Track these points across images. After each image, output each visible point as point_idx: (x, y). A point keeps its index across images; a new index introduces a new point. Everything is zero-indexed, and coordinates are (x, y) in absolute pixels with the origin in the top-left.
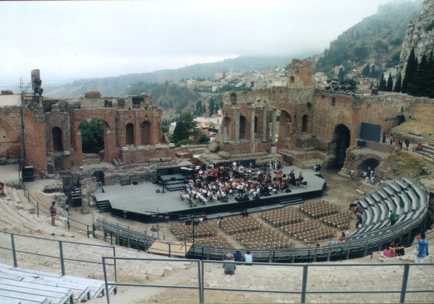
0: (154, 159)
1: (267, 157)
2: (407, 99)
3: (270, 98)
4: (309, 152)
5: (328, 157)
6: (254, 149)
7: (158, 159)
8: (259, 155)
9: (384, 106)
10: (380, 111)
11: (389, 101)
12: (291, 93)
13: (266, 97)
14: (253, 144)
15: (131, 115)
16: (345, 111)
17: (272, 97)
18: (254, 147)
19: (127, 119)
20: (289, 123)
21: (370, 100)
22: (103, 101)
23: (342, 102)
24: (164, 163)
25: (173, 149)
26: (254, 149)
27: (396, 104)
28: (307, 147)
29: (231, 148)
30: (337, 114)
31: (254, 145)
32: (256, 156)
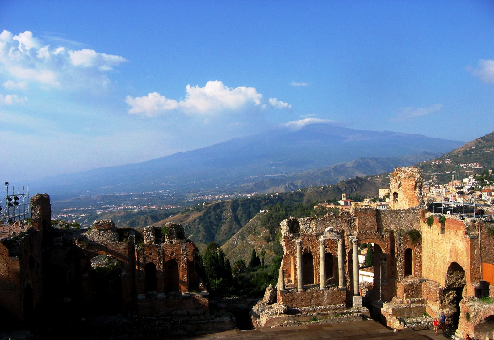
1: (345, 311)
3: (350, 226)
4: (414, 305)
5: (440, 312)
6: (325, 300)
8: (335, 309)
13: (344, 224)
14: (323, 291)
16: (456, 241)
17: (353, 225)
20: (383, 262)
23: (453, 228)
24: (193, 318)
26: (325, 300)
28: (412, 296)
29: (291, 298)
30: (448, 248)
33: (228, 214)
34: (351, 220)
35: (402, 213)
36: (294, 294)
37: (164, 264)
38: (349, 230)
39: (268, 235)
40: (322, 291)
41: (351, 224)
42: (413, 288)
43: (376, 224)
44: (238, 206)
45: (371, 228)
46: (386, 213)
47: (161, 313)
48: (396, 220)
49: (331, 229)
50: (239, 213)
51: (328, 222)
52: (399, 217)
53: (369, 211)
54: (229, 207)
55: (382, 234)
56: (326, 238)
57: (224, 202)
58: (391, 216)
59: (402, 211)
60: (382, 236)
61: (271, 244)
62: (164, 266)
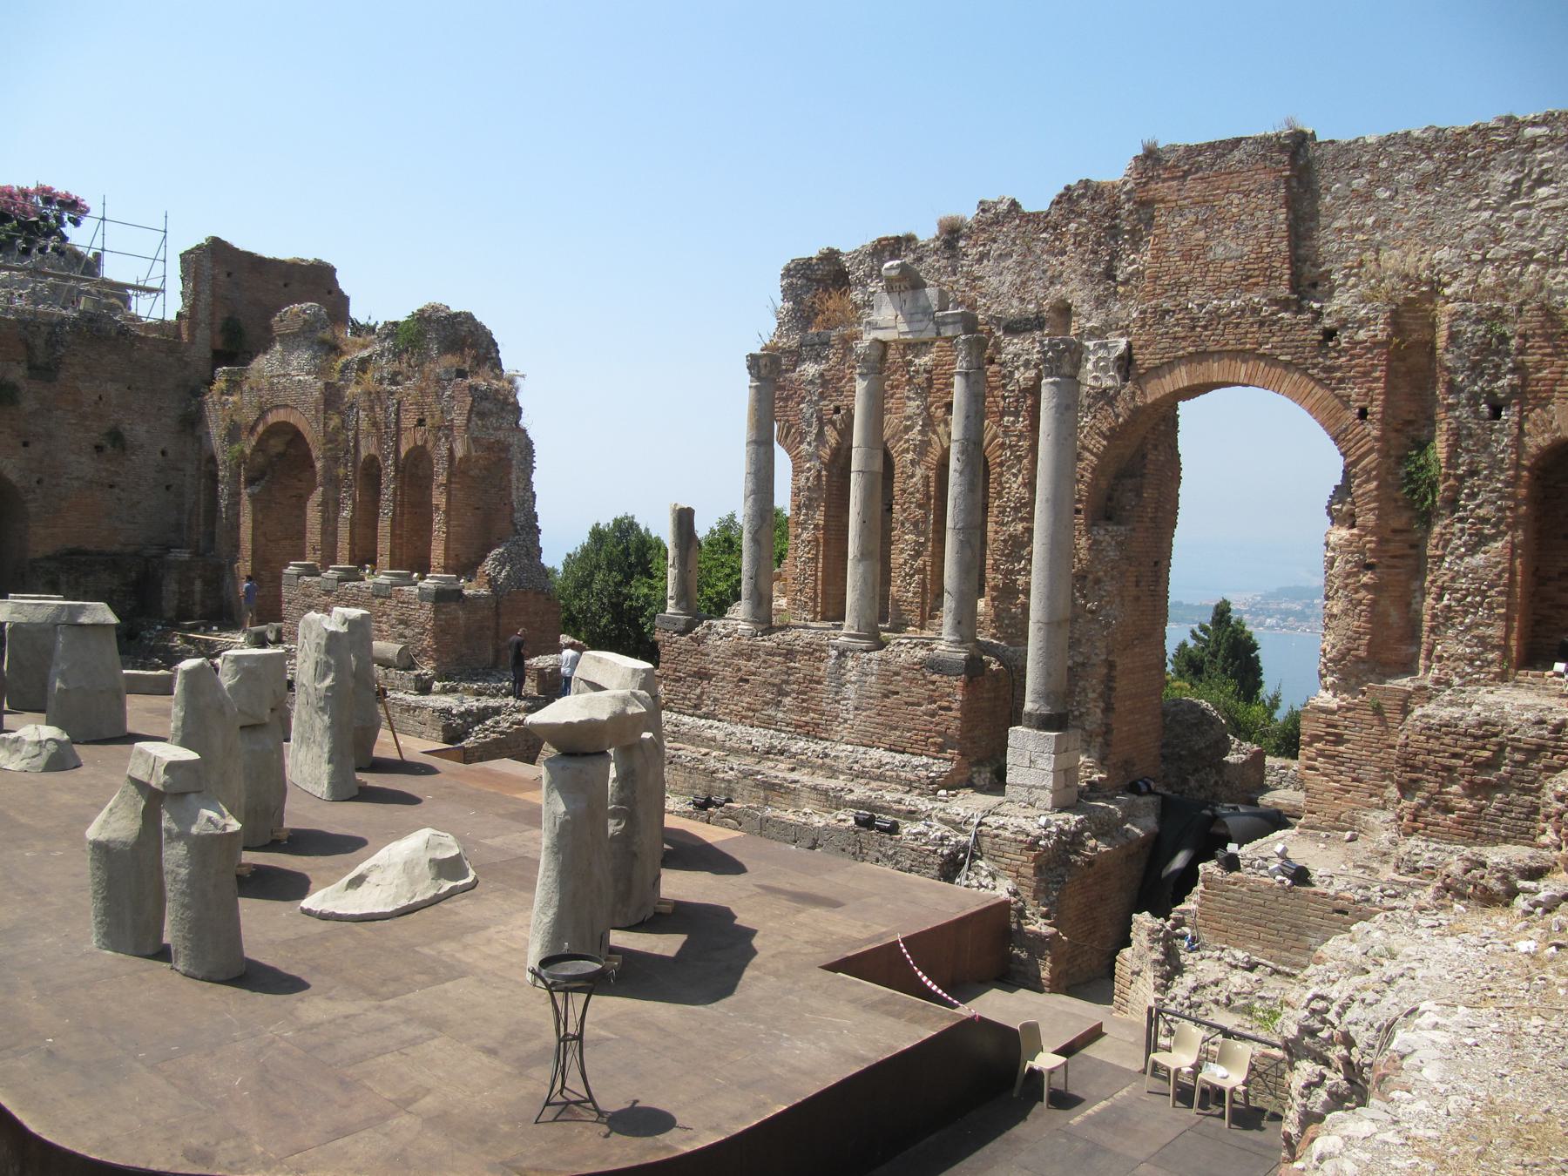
3: (1109, 274)
12: (1366, 197)
17: (1124, 270)
18: (850, 691)
29: (692, 664)
31: (852, 676)
32: (833, 773)
35: (1534, 144)
36: (712, 640)
37: (396, 463)
38: (1100, 303)
40: (834, 653)
41: (1115, 256)
43: (1284, 246)
45: (1245, 281)
46: (1383, 165)
48: (1475, 202)
49: (891, 268)
52: (1502, 178)
56: (880, 335)
59: (1529, 132)
62: (396, 470)
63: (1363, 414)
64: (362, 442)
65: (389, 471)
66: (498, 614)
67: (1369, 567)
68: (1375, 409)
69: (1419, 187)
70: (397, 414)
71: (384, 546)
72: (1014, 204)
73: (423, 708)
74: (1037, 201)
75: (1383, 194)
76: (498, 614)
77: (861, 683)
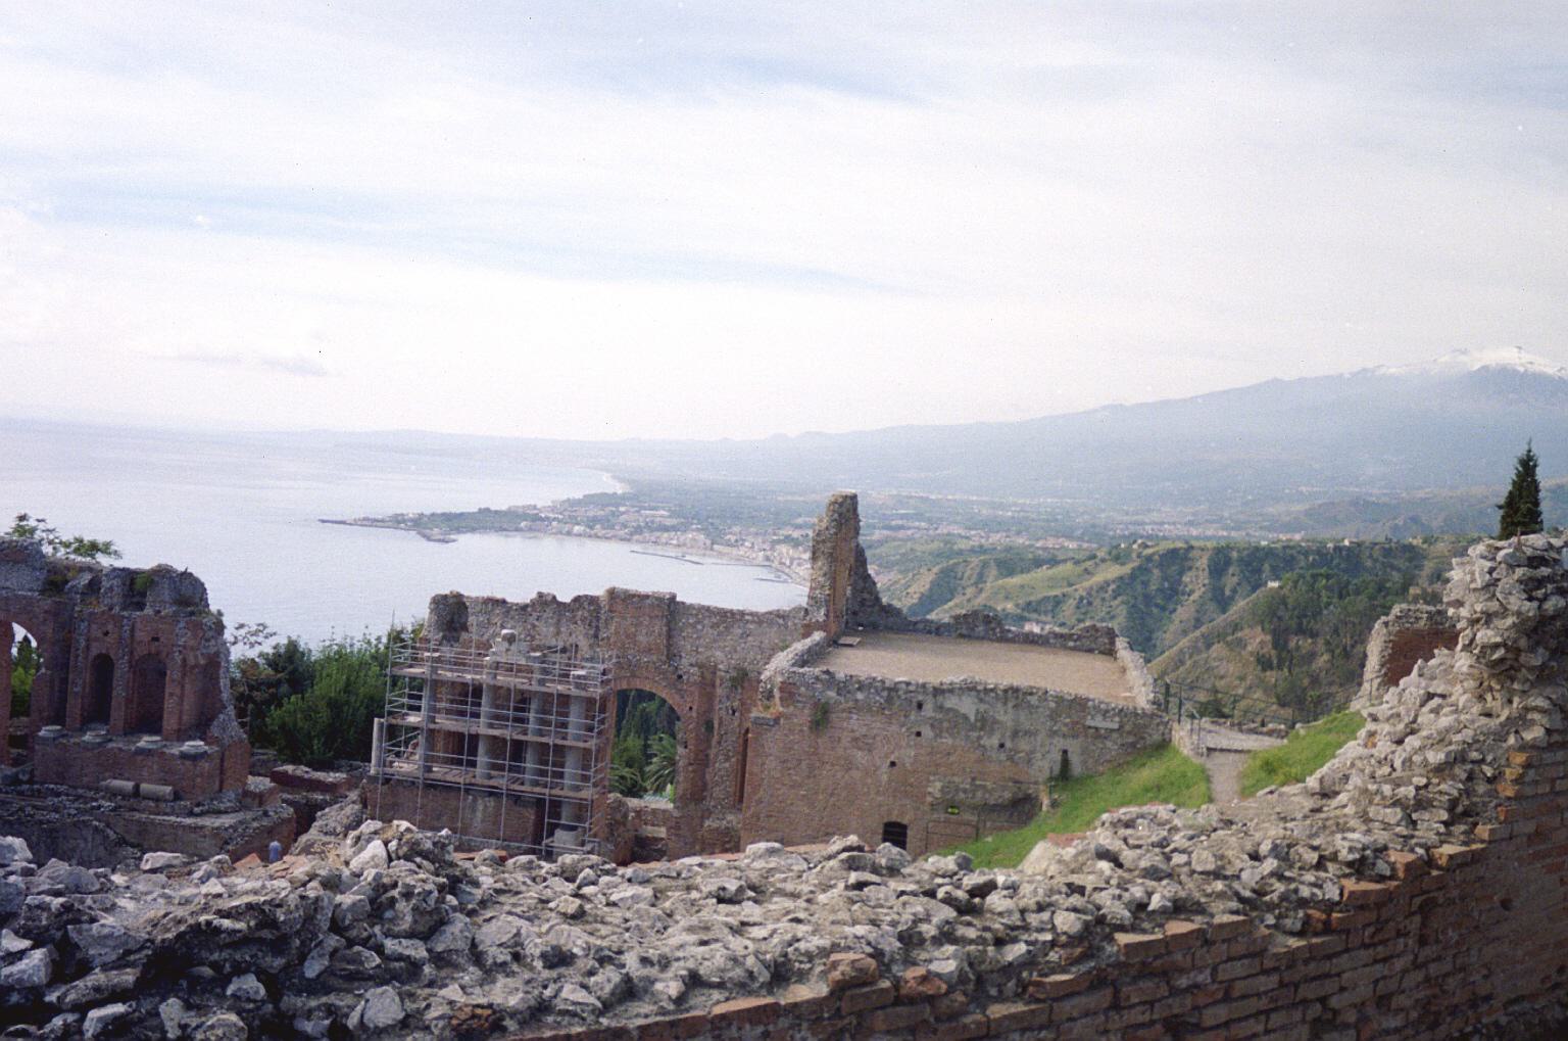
0: (117, 783)
2: (1098, 722)
3: (596, 636)
7: (129, 785)
9: (927, 732)
10: (907, 754)
11: (966, 718)
12: (693, 626)
15: (110, 627)
17: (602, 635)
18: (479, 815)
19: (97, 639)
21: (832, 694)
22: (42, 575)
25: (188, 763)
27: (1015, 734)
31: (481, 808)
33: (1197, 582)
34: (598, 619)
35: (748, 621)
38: (591, 646)
39: (1268, 650)
41: (597, 627)
42: (728, 842)
44: (1228, 562)
47: (85, 779)
50: (1230, 581)
51: (535, 615)
53: (648, 601)
54: (1203, 562)
55: (680, 672)
57: (1192, 547)
58: (714, 626)
60: (680, 677)
61: (1271, 676)
62: (131, 667)
63: (691, 708)
64: (94, 644)
65: (122, 669)
66: (222, 760)
67: (691, 764)
68: (695, 708)
69: (712, 627)
70: (132, 630)
71: (118, 714)
72: (554, 597)
73: (202, 827)
74: (565, 597)
75: (699, 627)
76: (222, 760)
77: (484, 810)
